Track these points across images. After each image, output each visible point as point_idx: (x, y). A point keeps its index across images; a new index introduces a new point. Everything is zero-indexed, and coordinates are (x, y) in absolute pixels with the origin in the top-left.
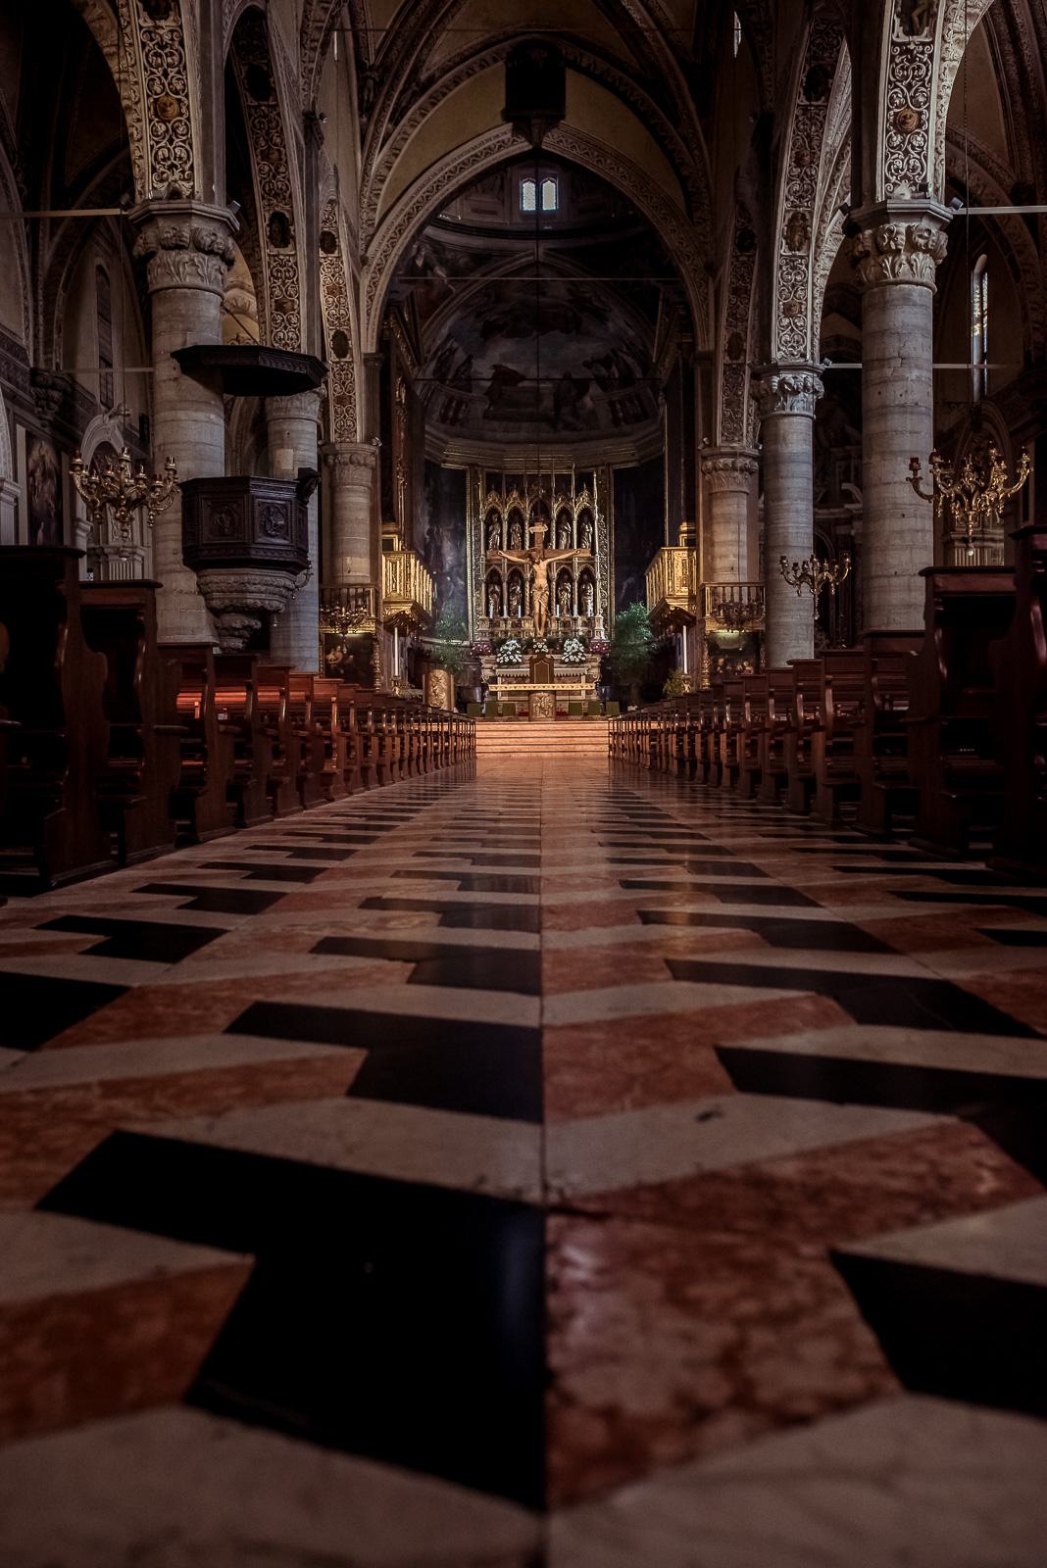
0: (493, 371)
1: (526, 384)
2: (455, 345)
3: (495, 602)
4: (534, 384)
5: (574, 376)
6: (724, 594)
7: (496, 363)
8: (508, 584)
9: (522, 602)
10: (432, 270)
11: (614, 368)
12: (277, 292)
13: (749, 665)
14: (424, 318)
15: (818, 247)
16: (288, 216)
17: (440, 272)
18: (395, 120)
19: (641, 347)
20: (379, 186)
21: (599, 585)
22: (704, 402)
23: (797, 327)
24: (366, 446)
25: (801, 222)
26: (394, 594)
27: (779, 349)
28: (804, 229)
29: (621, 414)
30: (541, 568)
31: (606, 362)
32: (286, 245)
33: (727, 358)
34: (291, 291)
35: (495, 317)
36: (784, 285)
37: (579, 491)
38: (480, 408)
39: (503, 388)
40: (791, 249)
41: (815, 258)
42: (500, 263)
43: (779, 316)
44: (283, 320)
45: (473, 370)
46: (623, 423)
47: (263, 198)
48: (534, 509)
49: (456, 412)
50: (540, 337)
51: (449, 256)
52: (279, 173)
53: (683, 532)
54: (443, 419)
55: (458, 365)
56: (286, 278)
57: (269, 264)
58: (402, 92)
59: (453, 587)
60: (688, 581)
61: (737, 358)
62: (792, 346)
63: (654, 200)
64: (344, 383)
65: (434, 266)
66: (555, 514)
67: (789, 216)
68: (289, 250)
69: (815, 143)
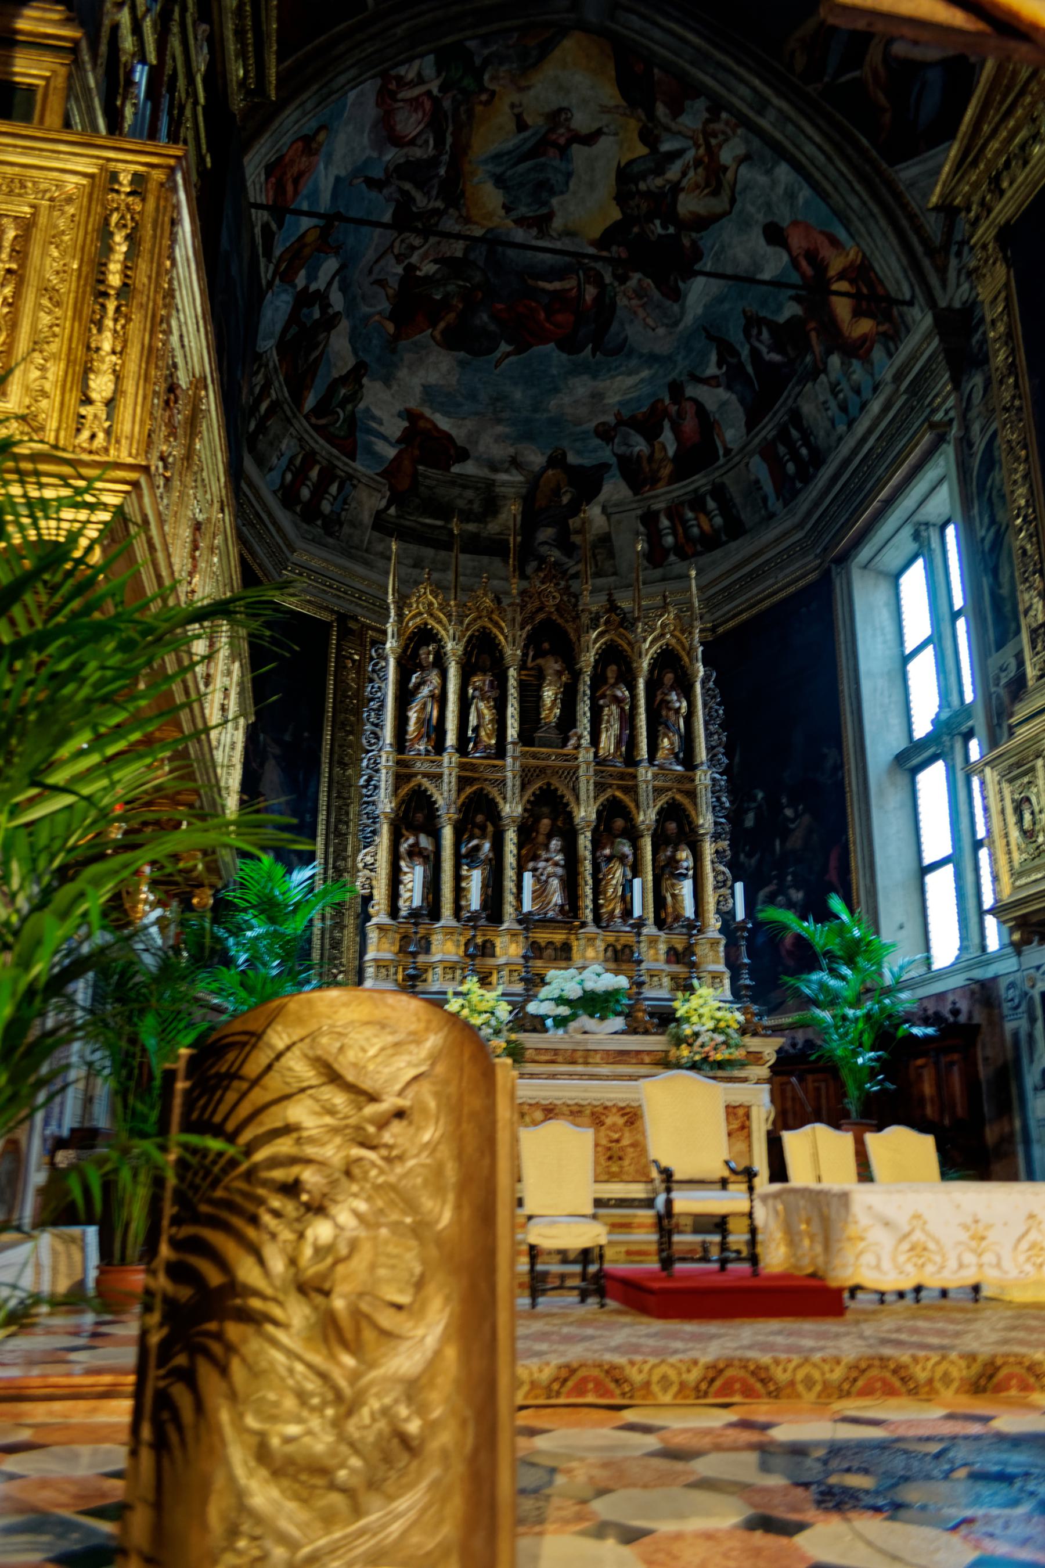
0: (406, 424)
1: (469, 468)
4: (485, 473)
5: (572, 459)
7: (412, 404)
11: (667, 437)
21: (708, 849)
29: (670, 540)
39: (421, 468)
45: (361, 406)
46: (672, 558)
48: (533, 642)
49: (319, 491)
66: (588, 659)
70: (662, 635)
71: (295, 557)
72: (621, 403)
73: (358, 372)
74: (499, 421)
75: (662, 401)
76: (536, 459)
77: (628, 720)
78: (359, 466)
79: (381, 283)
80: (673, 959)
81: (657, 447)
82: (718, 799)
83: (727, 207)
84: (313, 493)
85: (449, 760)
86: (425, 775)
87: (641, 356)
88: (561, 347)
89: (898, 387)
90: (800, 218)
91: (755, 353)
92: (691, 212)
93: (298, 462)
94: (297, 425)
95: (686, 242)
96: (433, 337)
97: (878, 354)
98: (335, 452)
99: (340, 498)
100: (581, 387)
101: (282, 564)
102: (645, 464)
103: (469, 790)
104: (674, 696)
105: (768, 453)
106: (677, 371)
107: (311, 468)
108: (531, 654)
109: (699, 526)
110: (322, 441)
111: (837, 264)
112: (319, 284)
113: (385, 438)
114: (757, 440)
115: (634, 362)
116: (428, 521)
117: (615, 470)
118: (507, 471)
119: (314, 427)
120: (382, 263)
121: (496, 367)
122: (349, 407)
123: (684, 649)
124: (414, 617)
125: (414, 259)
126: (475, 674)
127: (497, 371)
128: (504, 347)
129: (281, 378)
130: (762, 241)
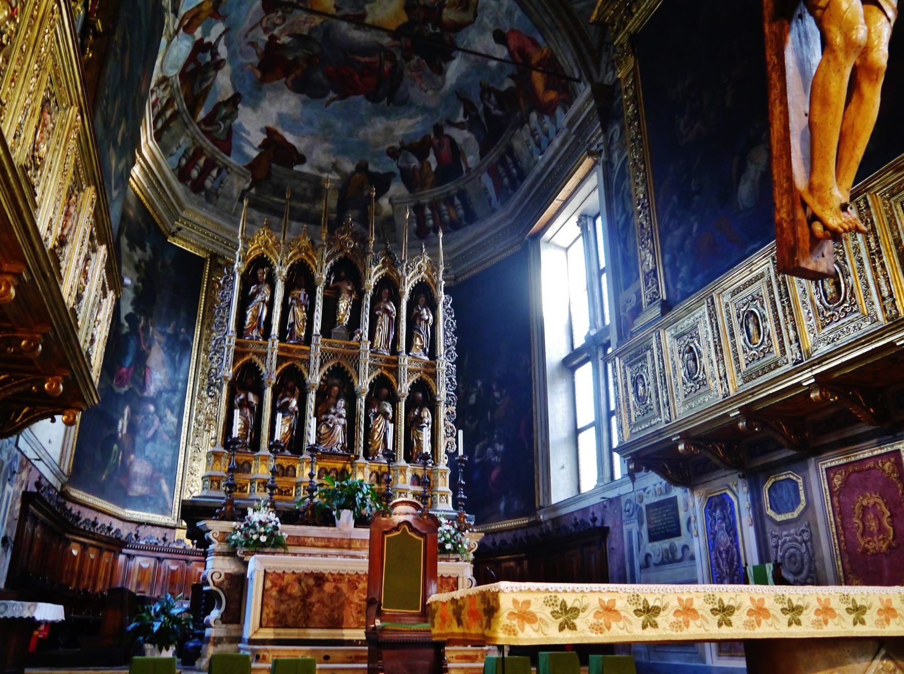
0: (265, 136)
1: (305, 168)
4: (315, 172)
5: (372, 168)
7: (271, 124)
11: (432, 159)
21: (442, 411)
29: (431, 222)
31: (420, 148)
38: (238, 184)
39: (274, 165)
45: (236, 122)
49: (205, 173)
55: (220, 99)
59: (156, 422)
66: (371, 283)
70: (420, 272)
71: (184, 214)
72: (405, 136)
73: (235, 100)
74: (326, 140)
75: (430, 136)
76: (349, 167)
77: (396, 324)
78: (232, 160)
79: (253, 44)
80: (416, 482)
81: (425, 165)
82: (450, 379)
83: (472, 18)
84: (200, 175)
85: (274, 345)
86: (255, 353)
87: (417, 107)
88: (368, 98)
89: (570, 130)
90: (516, 28)
91: (486, 110)
92: (450, 20)
93: (191, 152)
94: (191, 128)
95: (447, 38)
96: (286, 83)
97: (559, 111)
98: (216, 149)
99: (219, 179)
100: (379, 124)
101: (175, 217)
102: (417, 173)
103: (284, 365)
105: (493, 172)
106: (439, 118)
107: (200, 158)
108: (332, 278)
109: (449, 215)
110: (208, 141)
111: (536, 57)
112: (211, 38)
113: (251, 145)
114: (486, 164)
115: (413, 110)
117: (399, 177)
118: (329, 172)
119: (204, 132)
120: (254, 31)
121: (326, 106)
122: (228, 122)
123: (433, 282)
124: (255, 249)
125: (276, 32)
126: (293, 289)
127: (327, 109)
128: (332, 95)
129: (182, 96)
130: (492, 41)
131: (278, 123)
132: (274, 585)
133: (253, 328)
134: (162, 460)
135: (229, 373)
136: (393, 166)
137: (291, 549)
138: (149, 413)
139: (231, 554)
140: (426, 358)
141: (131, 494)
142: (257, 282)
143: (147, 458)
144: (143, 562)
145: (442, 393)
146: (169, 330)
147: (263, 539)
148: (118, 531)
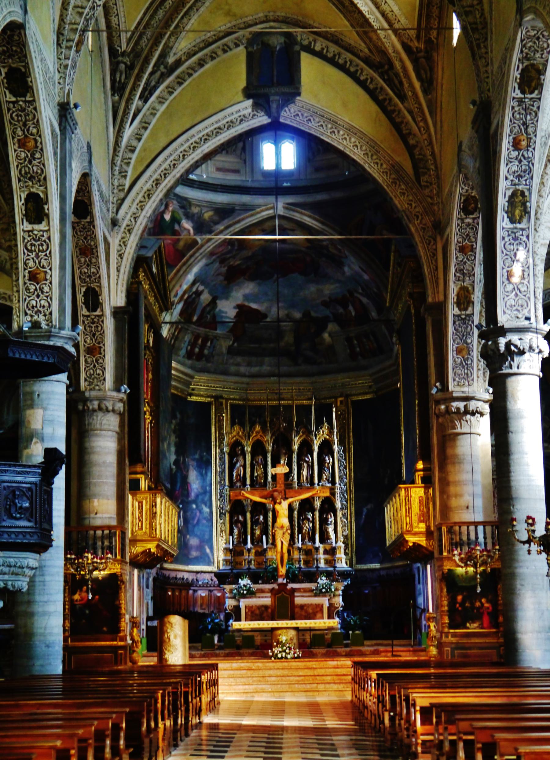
0: (237, 310)
2: (201, 288)
3: (239, 531)
5: (313, 314)
6: (460, 533)
7: (239, 302)
8: (251, 513)
9: (265, 531)
10: (179, 223)
11: (351, 308)
12: (31, 263)
13: (487, 602)
14: (171, 266)
15: (537, 219)
16: (42, 195)
17: (187, 225)
18: (145, 98)
19: (375, 290)
20: (129, 155)
21: (339, 514)
22: (435, 349)
23: (520, 292)
24: (115, 394)
25: (521, 198)
26: (140, 532)
27: (504, 313)
28: (524, 204)
29: (358, 349)
30: (283, 508)
31: (343, 301)
32: (40, 222)
33: (456, 309)
34: (44, 262)
35: (238, 262)
36: (506, 255)
37: (319, 425)
38: (224, 345)
39: (247, 325)
40: (512, 222)
41: (535, 230)
42: (242, 216)
43: (503, 283)
44: (36, 289)
45: (217, 310)
46: (360, 358)
47: (19, 180)
50: (280, 280)
51: (195, 210)
52: (34, 159)
53: (420, 470)
54: (190, 355)
55: (204, 305)
56: (39, 251)
57: (24, 238)
58: (151, 74)
59: (198, 514)
60: (424, 517)
61: (466, 309)
62: (517, 310)
63: (384, 166)
64: (94, 335)
65: (181, 220)
67: (509, 193)
68: (43, 226)
69: (530, 130)
73: (213, 303)
82: (343, 495)
84: (200, 349)
98: (208, 330)
100: (313, 288)
104: (327, 458)
107: (198, 339)
116: (252, 346)
122: (212, 313)
131: (244, 300)
132: (249, 610)
133: (237, 481)
134: (204, 535)
135: (228, 508)
136: (327, 312)
137: (258, 595)
138: (193, 509)
139: (234, 597)
140: (330, 485)
141: (191, 557)
142: (237, 455)
143: (196, 536)
144: (203, 593)
145: (338, 505)
146: (197, 456)
147: (245, 592)
148: (187, 579)
